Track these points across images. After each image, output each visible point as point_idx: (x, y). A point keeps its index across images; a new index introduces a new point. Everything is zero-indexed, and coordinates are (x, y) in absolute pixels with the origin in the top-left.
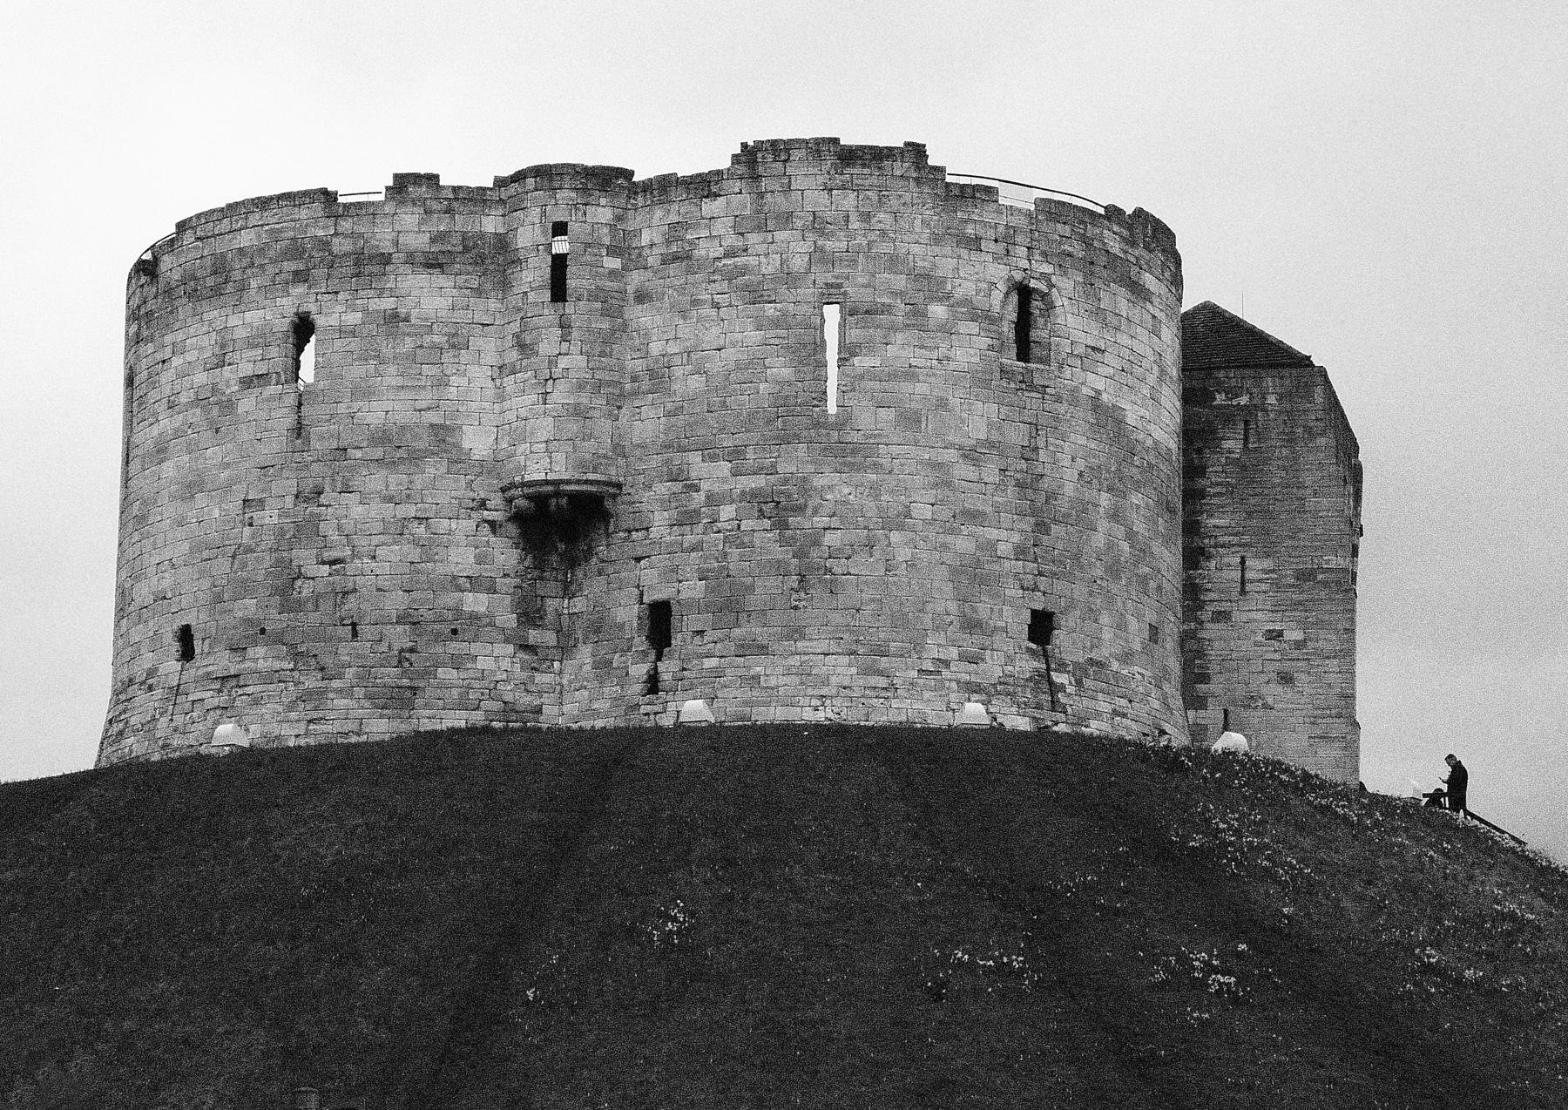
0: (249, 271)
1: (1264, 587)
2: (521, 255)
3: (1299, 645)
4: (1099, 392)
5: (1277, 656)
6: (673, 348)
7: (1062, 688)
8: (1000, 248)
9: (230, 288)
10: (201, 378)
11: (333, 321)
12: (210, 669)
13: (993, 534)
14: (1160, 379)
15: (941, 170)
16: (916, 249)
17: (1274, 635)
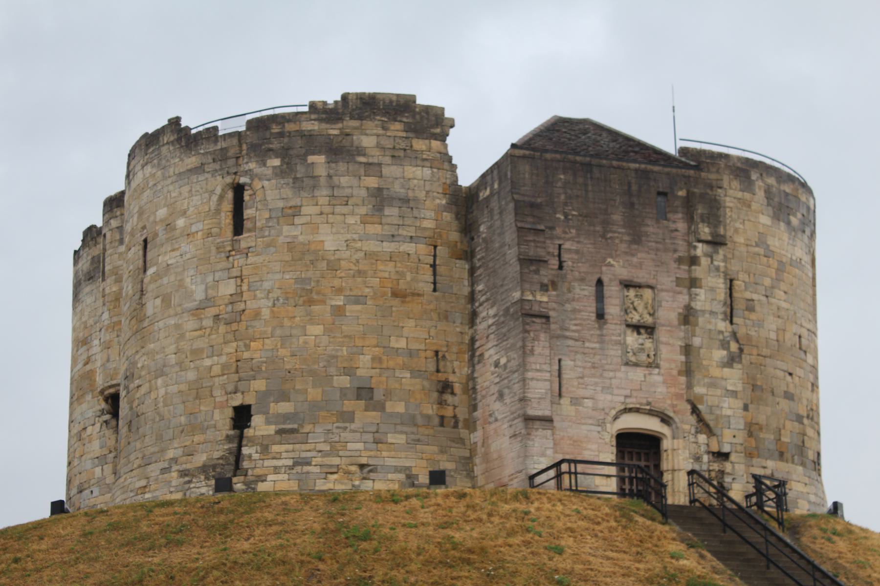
1: (494, 327)
3: (505, 365)
4: (295, 237)
5: (497, 380)
7: (250, 456)
8: (217, 166)
13: (208, 362)
14: (379, 208)
15: (187, 129)
16: (171, 188)
17: (497, 364)
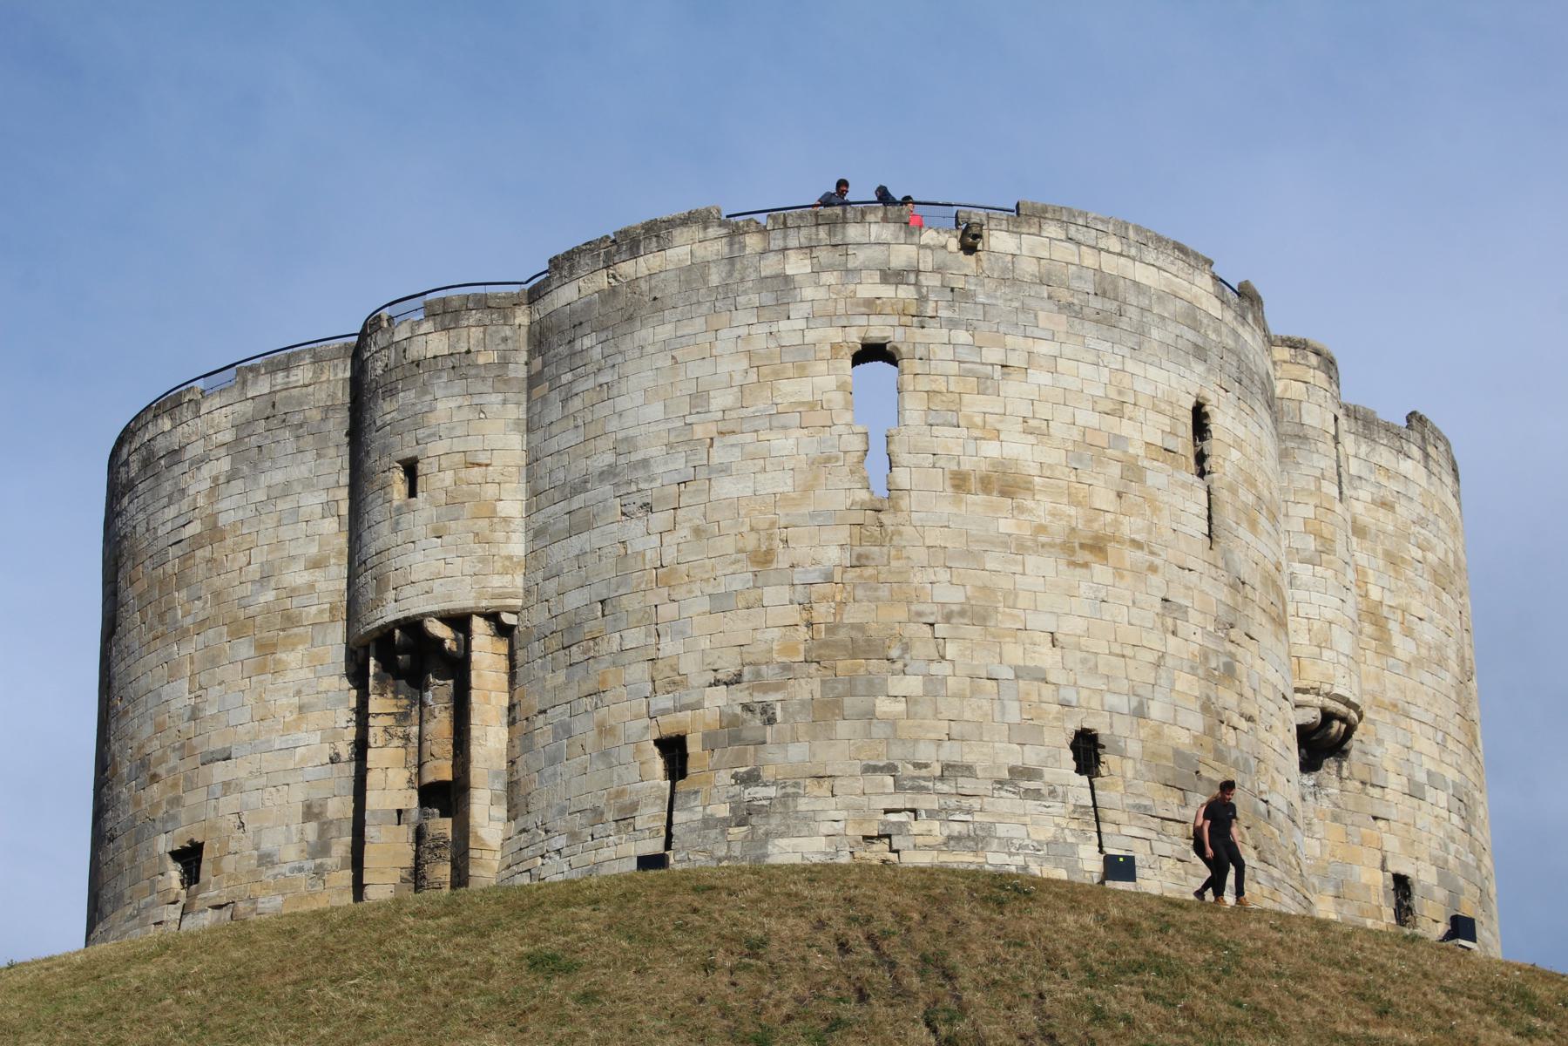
0: (1148, 318)
2: (1311, 433)
6: (1389, 600)
9: (1124, 323)
10: (1087, 418)
11: (1228, 423)
12: (1146, 802)
